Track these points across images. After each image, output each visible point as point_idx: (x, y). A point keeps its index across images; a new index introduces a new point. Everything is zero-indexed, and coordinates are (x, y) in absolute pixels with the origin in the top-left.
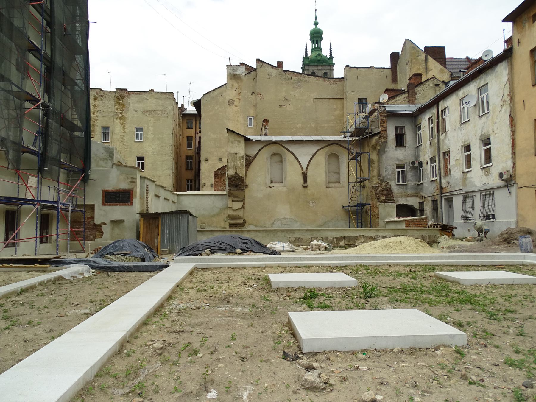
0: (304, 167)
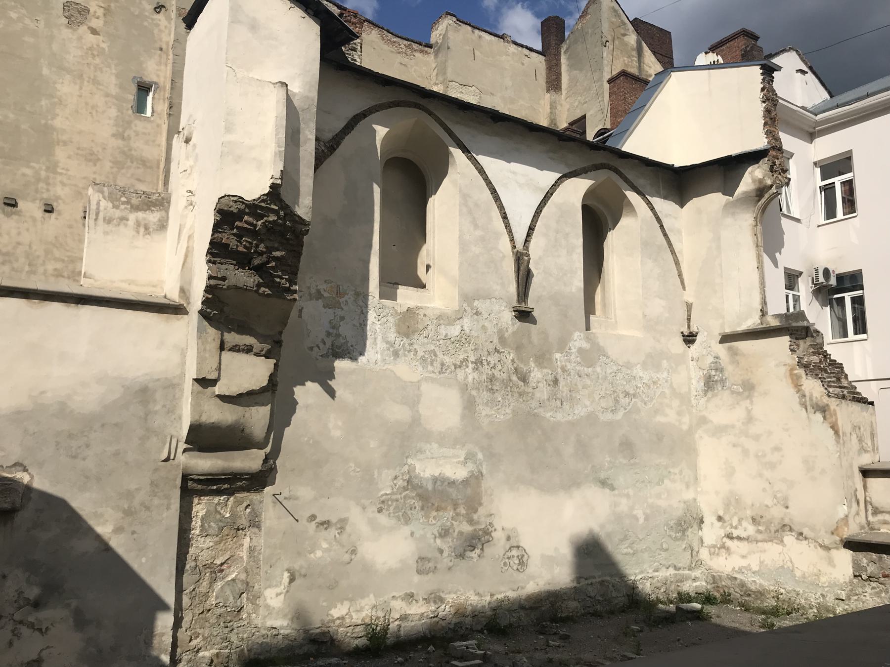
0: (520, 235)
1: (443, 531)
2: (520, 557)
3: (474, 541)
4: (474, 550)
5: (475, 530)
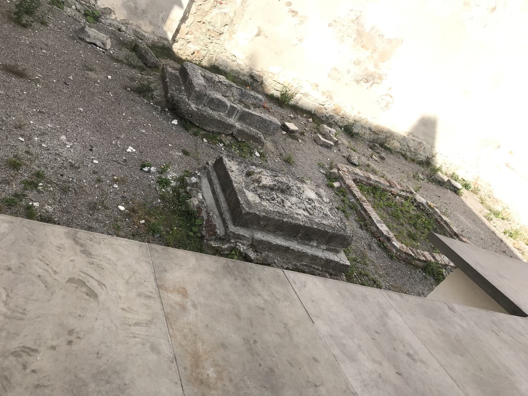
1: (357, 61)
2: (388, 103)
3: (370, 78)
4: (367, 83)
5: (375, 72)
